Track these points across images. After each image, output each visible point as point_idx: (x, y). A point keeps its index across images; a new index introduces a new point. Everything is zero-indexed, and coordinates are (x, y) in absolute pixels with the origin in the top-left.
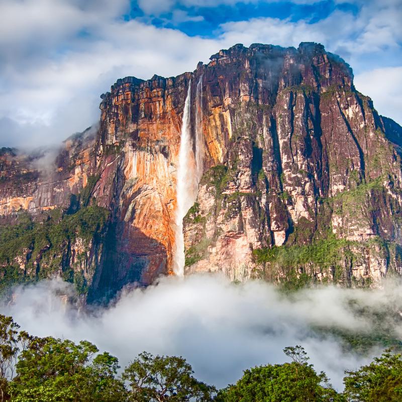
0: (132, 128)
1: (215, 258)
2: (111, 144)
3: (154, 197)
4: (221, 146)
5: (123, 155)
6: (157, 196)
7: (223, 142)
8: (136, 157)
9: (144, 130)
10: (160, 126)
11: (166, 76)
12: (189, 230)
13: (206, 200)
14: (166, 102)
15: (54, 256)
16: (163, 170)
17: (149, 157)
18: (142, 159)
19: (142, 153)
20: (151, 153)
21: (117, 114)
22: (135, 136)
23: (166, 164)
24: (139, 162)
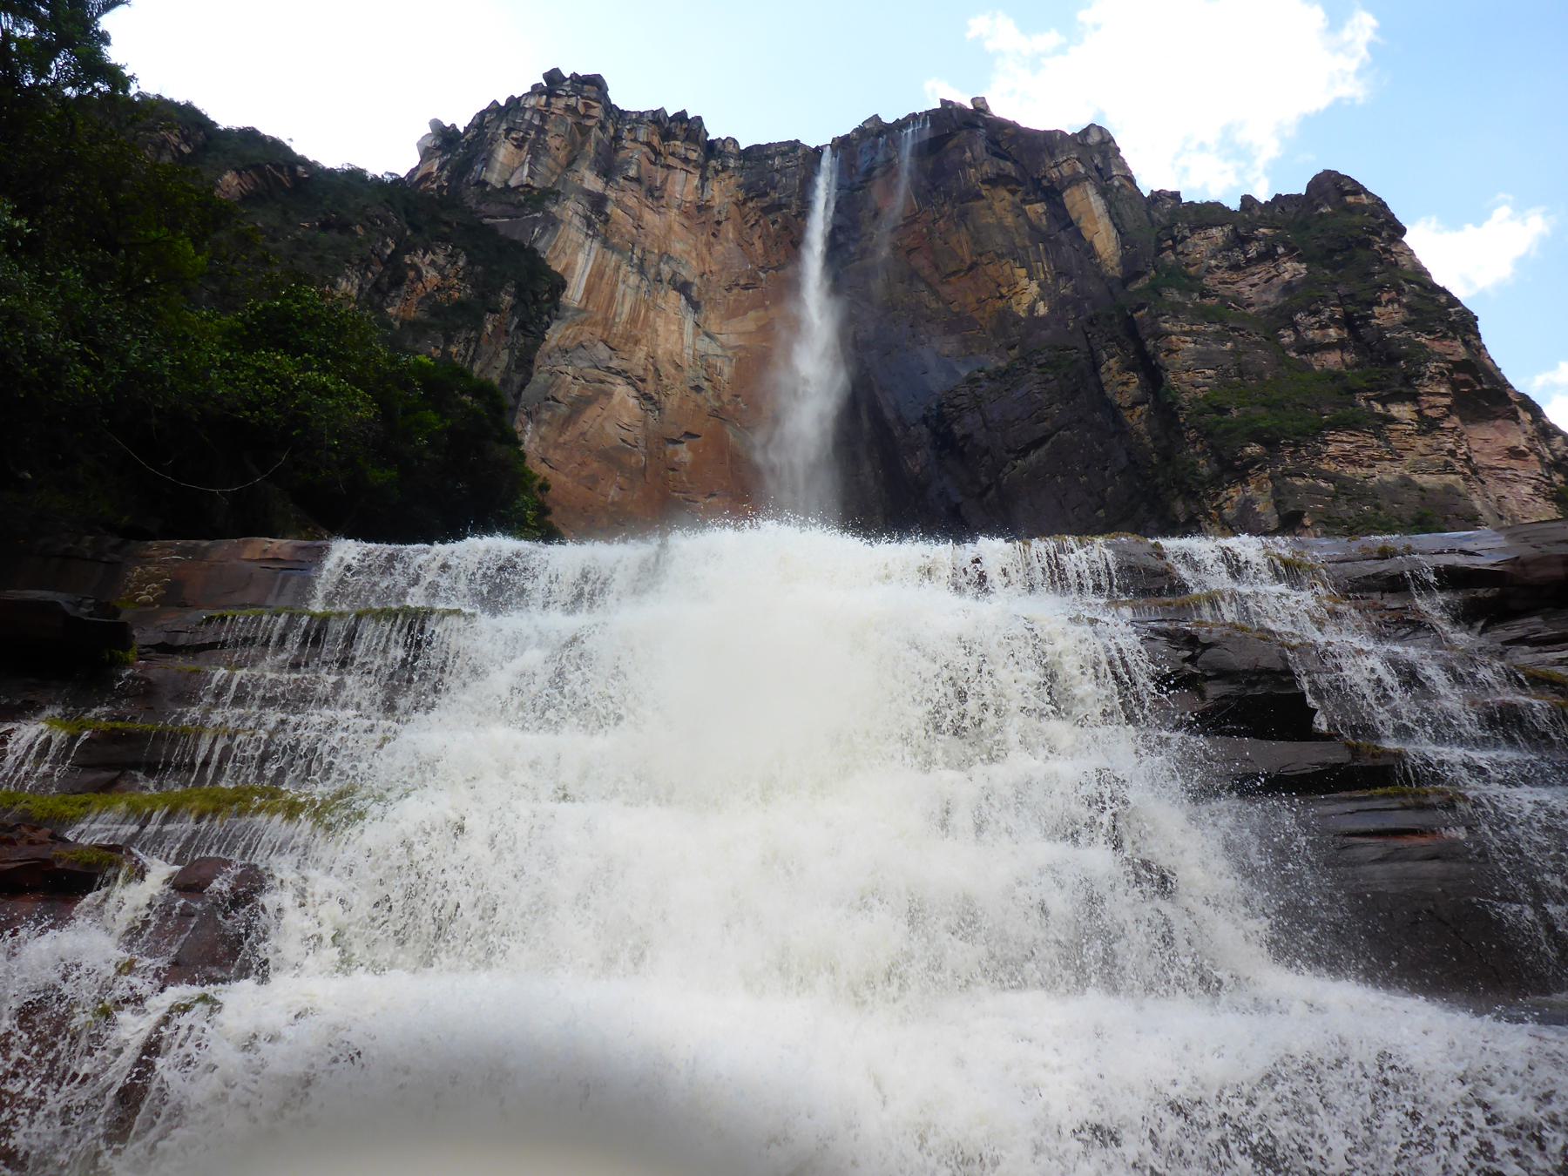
0: (593, 183)
1: (1420, 443)
2: (499, 186)
3: (623, 401)
4: (1030, 277)
5: (552, 223)
6: (632, 402)
7: (1044, 268)
8: (593, 255)
9: (626, 209)
10: (676, 227)
11: (715, 131)
12: (1186, 333)
13: (1235, 267)
14: (709, 184)
15: (325, 226)
16: (676, 335)
17: (633, 279)
18: (609, 272)
19: (613, 259)
20: (641, 270)
21: (541, 130)
22: (598, 203)
23: (689, 326)
24: (598, 274)
